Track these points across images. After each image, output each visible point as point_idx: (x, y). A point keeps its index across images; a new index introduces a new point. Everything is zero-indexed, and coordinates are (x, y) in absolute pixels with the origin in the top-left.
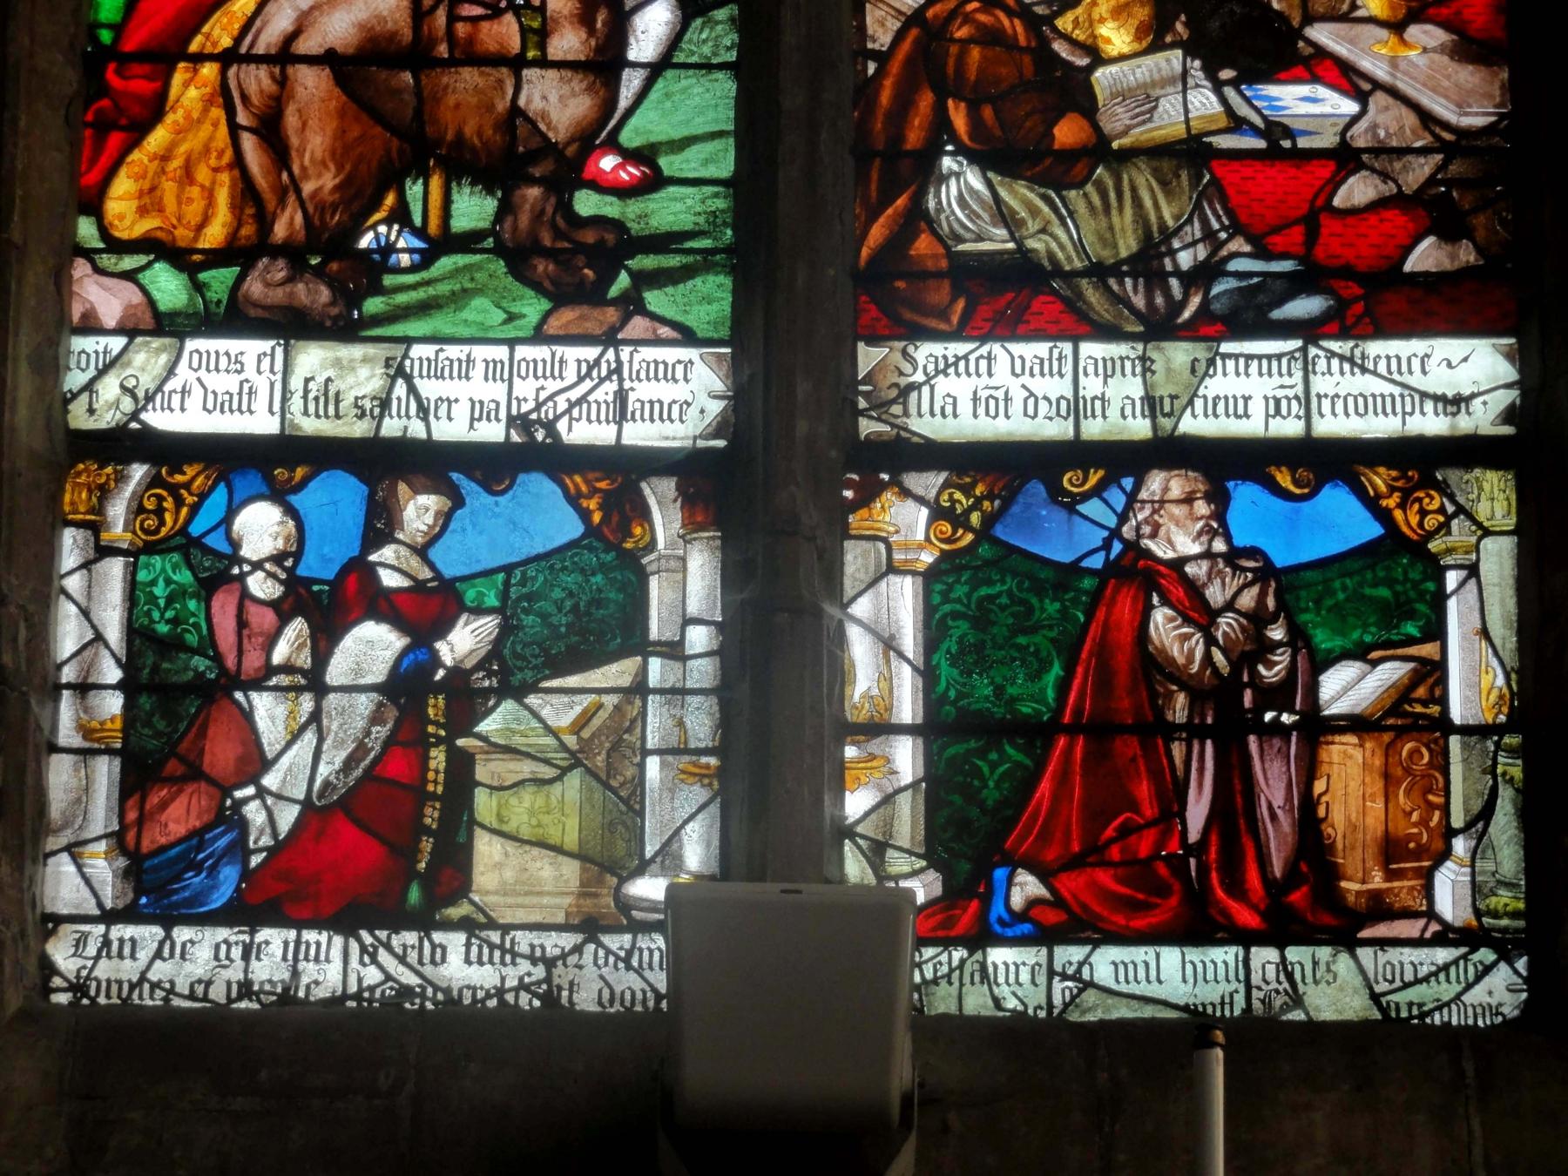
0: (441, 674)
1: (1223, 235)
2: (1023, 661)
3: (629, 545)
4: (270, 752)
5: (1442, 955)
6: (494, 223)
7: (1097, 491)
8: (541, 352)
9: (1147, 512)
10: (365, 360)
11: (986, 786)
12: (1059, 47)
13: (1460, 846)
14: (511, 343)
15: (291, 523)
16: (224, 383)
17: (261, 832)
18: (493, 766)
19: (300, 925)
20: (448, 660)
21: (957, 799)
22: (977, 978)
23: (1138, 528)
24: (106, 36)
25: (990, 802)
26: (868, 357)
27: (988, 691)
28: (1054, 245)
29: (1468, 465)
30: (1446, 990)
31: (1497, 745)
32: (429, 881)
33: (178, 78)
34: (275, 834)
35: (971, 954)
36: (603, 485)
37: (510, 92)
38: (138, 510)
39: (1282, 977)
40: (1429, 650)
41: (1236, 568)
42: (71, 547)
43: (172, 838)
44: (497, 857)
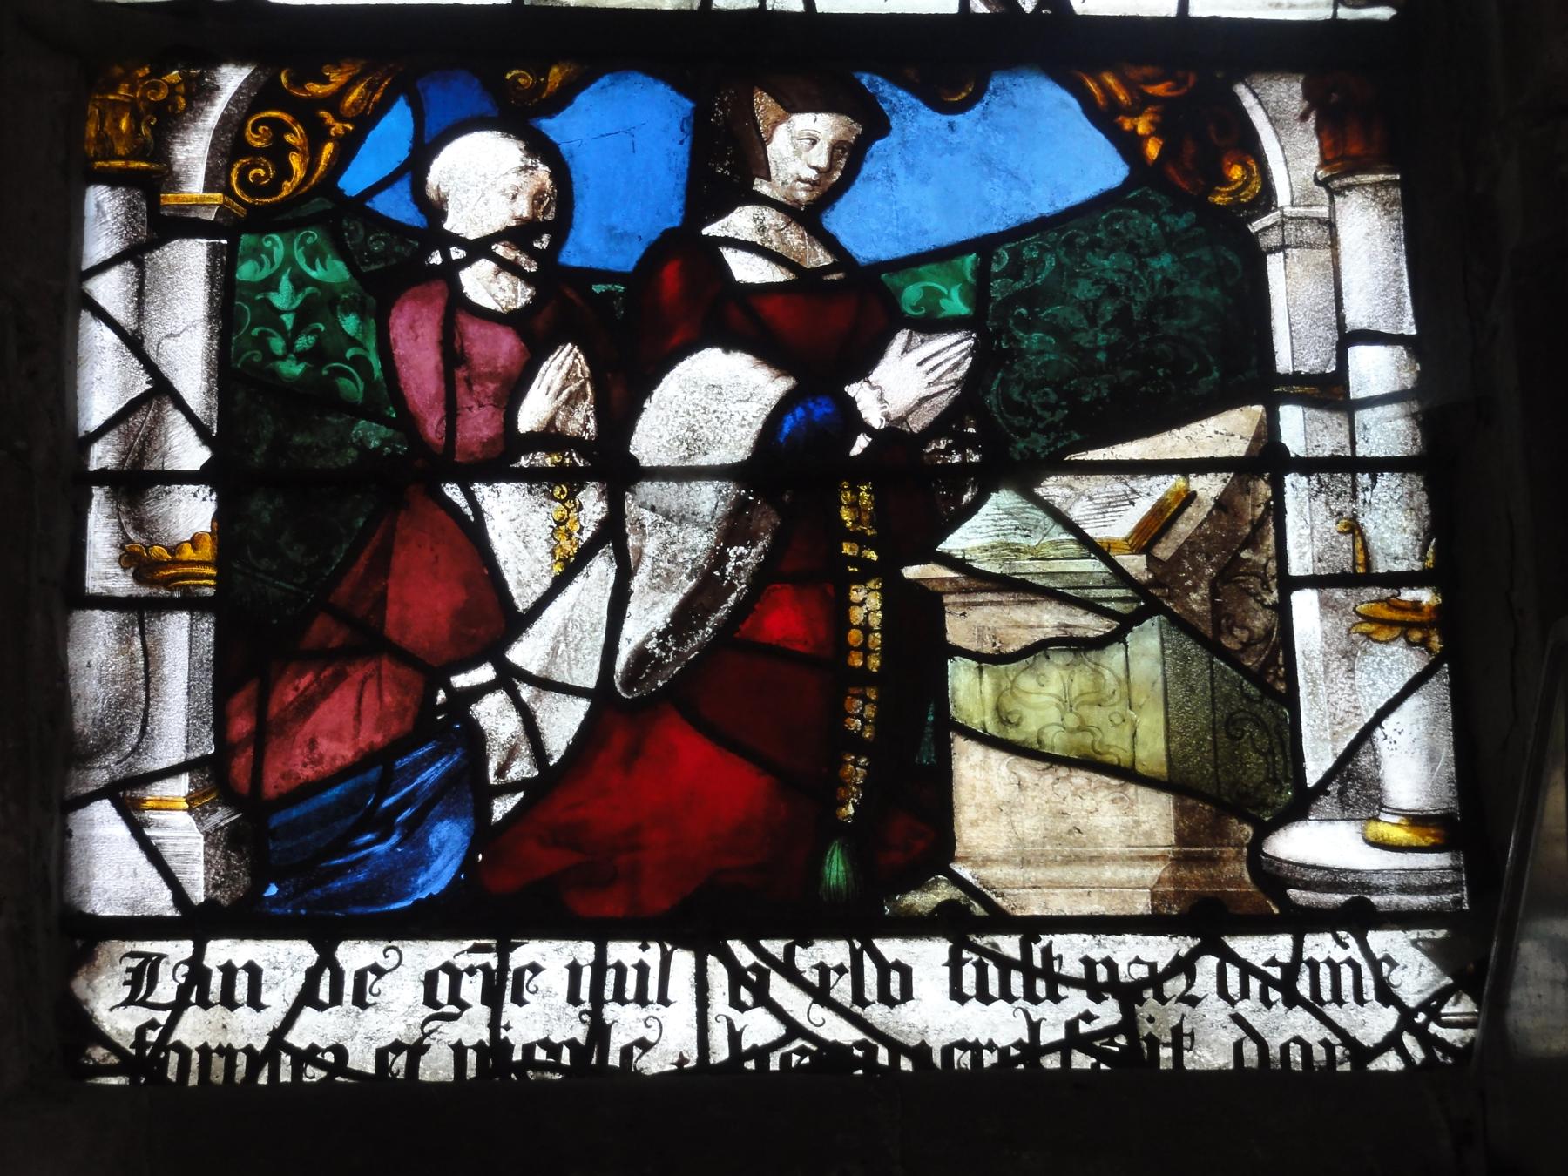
0: (862, 443)
4: (523, 599)
15: (543, 171)
17: (512, 754)
18: (977, 616)
19: (601, 935)
20: (875, 419)
32: (859, 841)
36: (1159, 90)
43: (325, 768)
44: (1003, 791)
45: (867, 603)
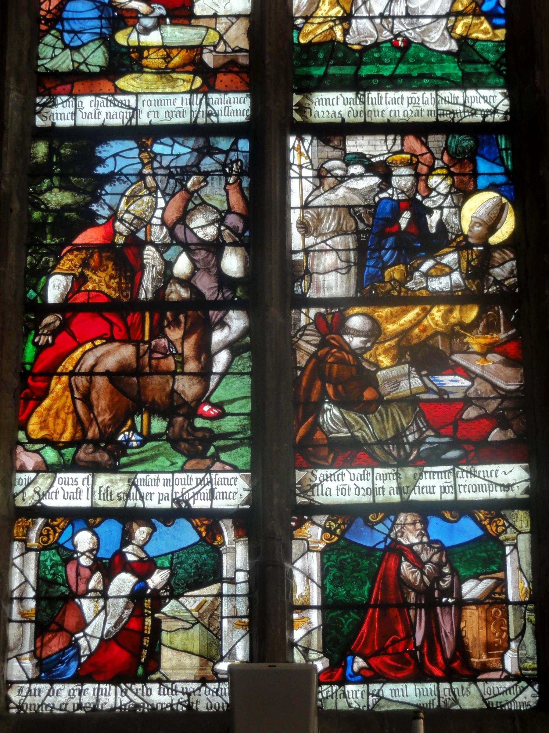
0: (149, 591)
1: (424, 429)
2: (356, 582)
3: (215, 544)
4: (88, 620)
5: (508, 684)
6: (166, 430)
7: (381, 521)
8: (183, 476)
9: (399, 528)
10: (121, 480)
11: (344, 627)
12: (365, 364)
13: (513, 645)
14: (173, 473)
15: (95, 538)
16: (71, 489)
17: (85, 649)
19: (99, 682)
21: (334, 632)
22: (342, 696)
23: (396, 534)
24: (28, 367)
25: (345, 633)
26: (299, 475)
27: (344, 593)
28: (364, 434)
30: (510, 697)
31: (526, 608)
32: (145, 666)
33: (54, 381)
34: (90, 649)
35: (340, 687)
36: (206, 522)
37: (171, 384)
38: (40, 534)
39: (451, 693)
40: (500, 575)
41: (432, 547)
42: (16, 548)
44: (170, 656)
45: (148, 621)
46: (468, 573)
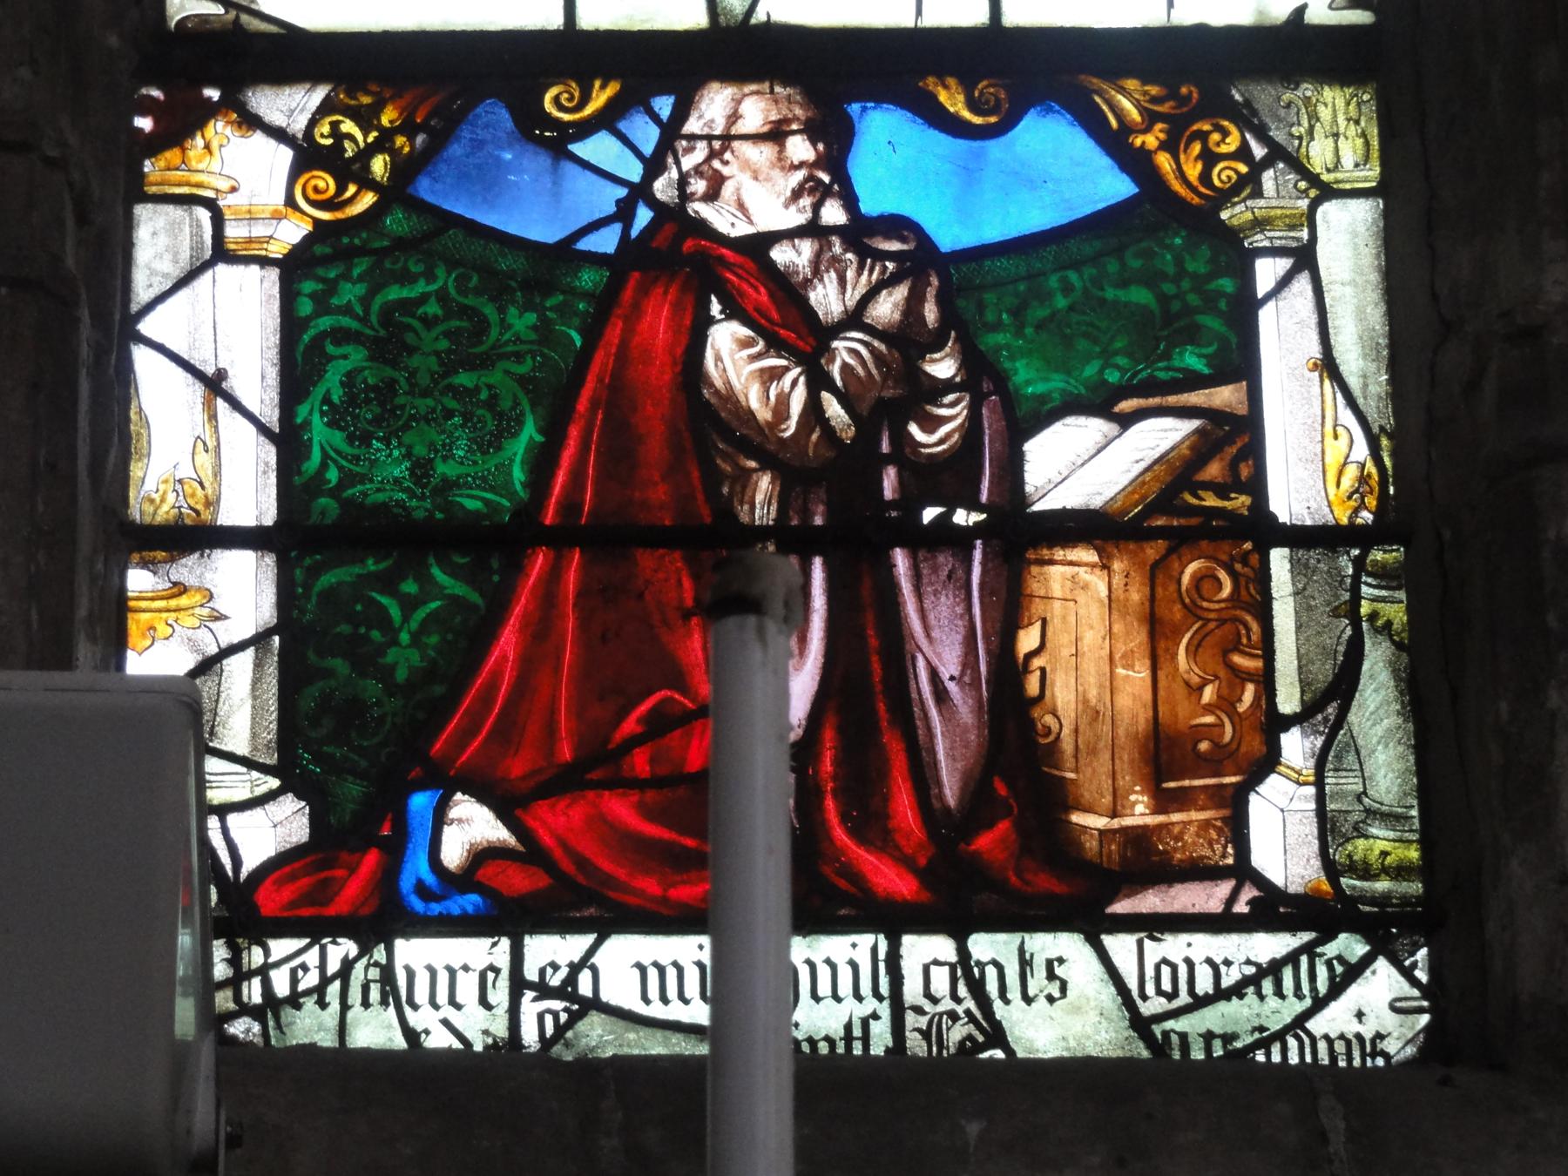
2: (467, 417)
5: (1269, 946)
7: (607, 120)
9: (700, 152)
11: (395, 642)
13: (1296, 747)
21: (339, 665)
22: (375, 995)
23: (683, 181)
25: (401, 675)
27: (400, 471)
29: (1290, 76)
30: (1278, 1011)
31: (1359, 564)
35: (365, 950)
39: (962, 990)
40: (1226, 396)
41: (866, 254)
46: (1055, 384)
